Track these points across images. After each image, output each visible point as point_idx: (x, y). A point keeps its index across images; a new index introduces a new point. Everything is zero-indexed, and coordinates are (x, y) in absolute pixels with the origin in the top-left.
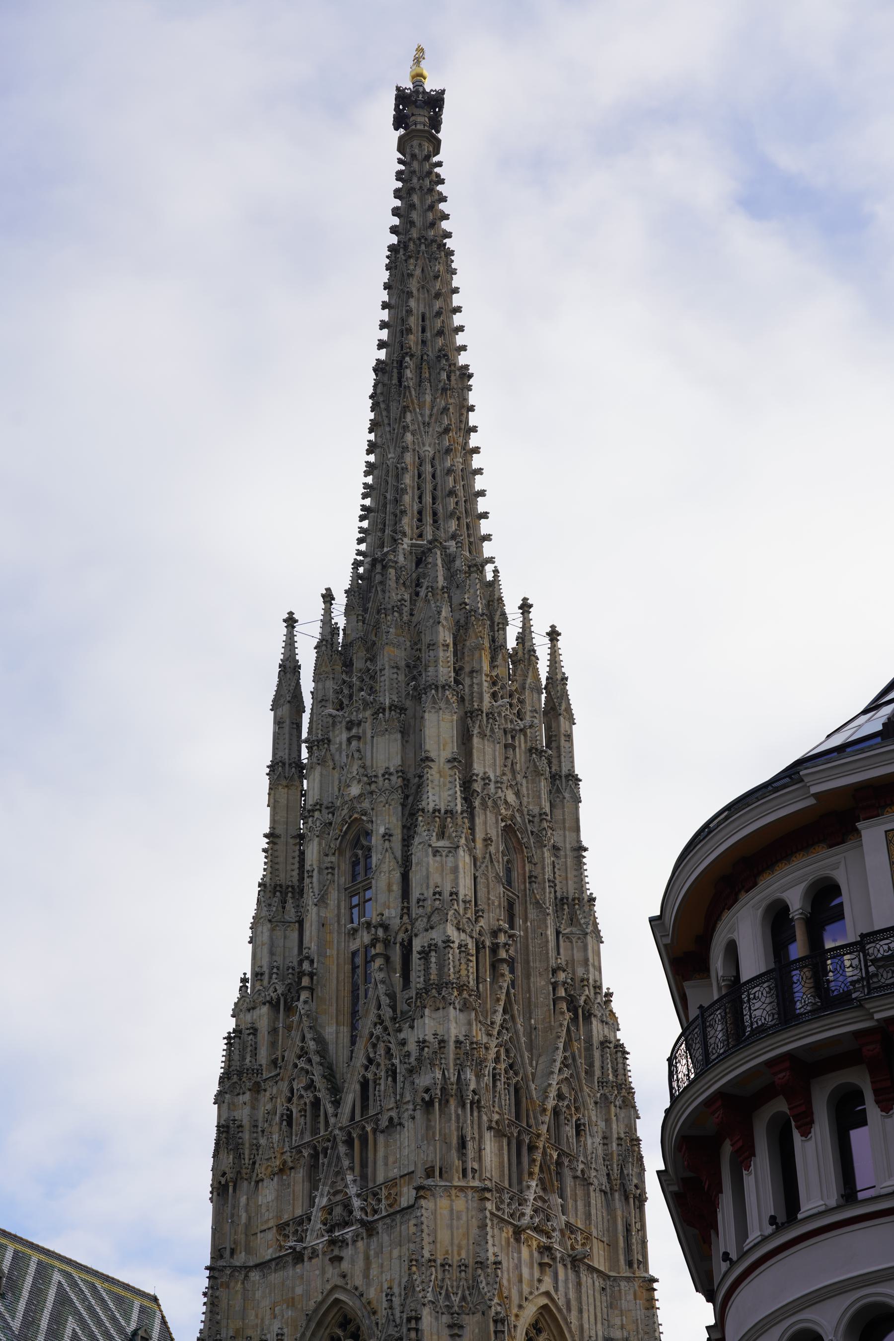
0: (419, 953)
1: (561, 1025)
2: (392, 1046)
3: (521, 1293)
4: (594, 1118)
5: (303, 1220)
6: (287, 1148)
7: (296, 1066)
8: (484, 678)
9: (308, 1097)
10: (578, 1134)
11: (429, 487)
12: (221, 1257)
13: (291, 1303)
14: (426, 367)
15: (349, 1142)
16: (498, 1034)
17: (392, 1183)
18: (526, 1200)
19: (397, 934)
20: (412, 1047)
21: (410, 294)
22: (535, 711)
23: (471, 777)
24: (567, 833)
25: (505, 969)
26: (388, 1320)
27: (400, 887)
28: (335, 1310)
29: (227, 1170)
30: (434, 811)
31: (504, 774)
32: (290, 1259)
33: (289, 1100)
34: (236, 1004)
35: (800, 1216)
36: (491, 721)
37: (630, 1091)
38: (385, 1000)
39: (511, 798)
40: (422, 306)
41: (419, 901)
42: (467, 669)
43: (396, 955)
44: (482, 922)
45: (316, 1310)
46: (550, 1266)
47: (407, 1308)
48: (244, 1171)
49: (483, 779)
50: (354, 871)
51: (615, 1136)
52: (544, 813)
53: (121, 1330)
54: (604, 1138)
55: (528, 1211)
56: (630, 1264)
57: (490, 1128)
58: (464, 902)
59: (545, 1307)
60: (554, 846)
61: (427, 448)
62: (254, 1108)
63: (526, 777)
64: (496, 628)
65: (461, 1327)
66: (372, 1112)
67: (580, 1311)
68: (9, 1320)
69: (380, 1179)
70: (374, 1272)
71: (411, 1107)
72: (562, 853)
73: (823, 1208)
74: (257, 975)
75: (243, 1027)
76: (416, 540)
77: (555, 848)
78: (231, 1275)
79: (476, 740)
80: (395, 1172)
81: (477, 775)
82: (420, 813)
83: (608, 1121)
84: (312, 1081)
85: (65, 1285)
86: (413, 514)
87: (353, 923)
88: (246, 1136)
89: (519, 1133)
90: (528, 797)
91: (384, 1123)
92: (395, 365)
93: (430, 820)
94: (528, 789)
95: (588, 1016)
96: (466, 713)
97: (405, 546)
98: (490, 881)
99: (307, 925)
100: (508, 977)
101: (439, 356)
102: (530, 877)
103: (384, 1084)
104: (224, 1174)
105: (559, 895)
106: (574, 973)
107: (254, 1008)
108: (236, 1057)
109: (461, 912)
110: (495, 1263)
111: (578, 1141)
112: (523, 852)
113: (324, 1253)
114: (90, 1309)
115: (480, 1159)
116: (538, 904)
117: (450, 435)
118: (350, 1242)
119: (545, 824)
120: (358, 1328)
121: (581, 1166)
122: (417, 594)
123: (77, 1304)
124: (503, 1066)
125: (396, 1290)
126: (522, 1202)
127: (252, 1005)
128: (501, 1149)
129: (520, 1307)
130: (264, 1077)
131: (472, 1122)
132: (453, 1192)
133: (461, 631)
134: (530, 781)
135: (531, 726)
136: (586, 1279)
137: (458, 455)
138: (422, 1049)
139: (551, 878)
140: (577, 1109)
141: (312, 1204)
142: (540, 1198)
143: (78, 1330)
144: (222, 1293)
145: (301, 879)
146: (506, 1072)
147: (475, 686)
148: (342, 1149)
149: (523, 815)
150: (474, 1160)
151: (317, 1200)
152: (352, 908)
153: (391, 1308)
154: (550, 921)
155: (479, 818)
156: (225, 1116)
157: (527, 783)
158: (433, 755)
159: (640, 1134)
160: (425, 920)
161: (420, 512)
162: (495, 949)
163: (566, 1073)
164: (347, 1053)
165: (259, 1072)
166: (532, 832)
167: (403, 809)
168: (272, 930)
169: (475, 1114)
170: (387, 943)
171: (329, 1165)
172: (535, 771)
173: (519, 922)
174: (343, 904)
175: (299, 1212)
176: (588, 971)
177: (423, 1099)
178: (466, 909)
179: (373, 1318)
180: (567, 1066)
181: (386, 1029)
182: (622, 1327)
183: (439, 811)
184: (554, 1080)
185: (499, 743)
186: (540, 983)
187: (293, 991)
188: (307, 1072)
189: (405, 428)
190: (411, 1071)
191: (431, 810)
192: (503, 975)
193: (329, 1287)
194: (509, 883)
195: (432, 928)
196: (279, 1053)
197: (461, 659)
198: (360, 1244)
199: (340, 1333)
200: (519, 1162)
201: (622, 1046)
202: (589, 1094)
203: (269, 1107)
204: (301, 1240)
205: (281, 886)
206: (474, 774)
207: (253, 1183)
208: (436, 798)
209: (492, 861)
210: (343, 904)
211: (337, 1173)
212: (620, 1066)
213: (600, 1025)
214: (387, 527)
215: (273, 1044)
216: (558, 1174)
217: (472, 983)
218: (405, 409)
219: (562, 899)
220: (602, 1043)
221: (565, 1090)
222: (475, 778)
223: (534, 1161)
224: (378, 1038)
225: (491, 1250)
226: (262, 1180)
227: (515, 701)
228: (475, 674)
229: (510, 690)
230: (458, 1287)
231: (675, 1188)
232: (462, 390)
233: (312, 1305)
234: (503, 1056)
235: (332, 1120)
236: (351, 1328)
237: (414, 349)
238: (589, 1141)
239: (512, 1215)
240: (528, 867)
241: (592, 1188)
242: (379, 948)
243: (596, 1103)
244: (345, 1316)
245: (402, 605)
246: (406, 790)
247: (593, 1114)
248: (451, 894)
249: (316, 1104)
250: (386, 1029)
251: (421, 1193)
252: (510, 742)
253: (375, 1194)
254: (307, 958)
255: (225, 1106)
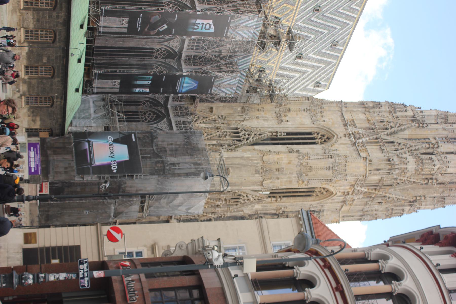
0: (431, 157)
1: (409, 198)
2: (404, 150)
3: (337, 186)
4: (383, 207)
5: (355, 126)
6: (374, 121)
7: (397, 123)
9: (388, 127)
10: (379, 203)
12: (344, 104)
13: (333, 124)
15: (377, 138)
16: (408, 180)
17: (366, 150)
18: (361, 188)
19: (436, 151)
20: (404, 155)
25: (426, 182)
26: (330, 150)
28: (332, 136)
29: (368, 105)
32: (344, 123)
33: (388, 122)
34: (413, 106)
35: (441, 274)
37: (390, 217)
38: (417, 148)
41: (446, 157)
43: (430, 151)
44: (440, 175)
45: (331, 130)
46: (344, 195)
47: (334, 155)
48: (368, 110)
50: (453, 138)
51: (378, 213)
53: (321, 80)
54: (377, 210)
55: (359, 188)
56: (343, 217)
57: (382, 178)
58: (446, 170)
59: (333, 193)
62: (385, 111)
65: (329, 170)
66: (385, 144)
67: (331, 203)
68: (325, 49)
69: (367, 147)
70: (342, 146)
71: (388, 155)
73: (445, 282)
74: (422, 112)
75: (407, 108)
78: (340, 107)
80: (369, 151)
83: (382, 211)
84: (393, 128)
85: (333, 64)
87: (438, 138)
88: (377, 110)
89: (380, 186)
91: (383, 148)
95: (411, 206)
99: (436, 125)
100: (424, 183)
103: (394, 148)
104: (367, 104)
105: (445, 198)
106: (423, 202)
107: (412, 111)
108: (399, 106)
109: (443, 169)
110: (346, 179)
111: (377, 203)
113: (347, 132)
114: (327, 71)
115: (374, 175)
116: (443, 191)
118: (350, 139)
120: (327, 142)
121: (370, 203)
123: (328, 67)
124: (399, 181)
125: (338, 152)
126: (361, 187)
127: (413, 110)
128: (376, 181)
129: (333, 186)
130: (394, 115)
131: (384, 173)
132: (365, 167)
136: (340, 205)
138: (404, 158)
140: (386, 202)
141: (361, 128)
142: (362, 192)
143: (322, 68)
144: (335, 105)
145: (449, 123)
146: (397, 182)
148: (375, 136)
150: (374, 173)
151: (361, 130)
152: (442, 138)
153: (333, 151)
154: (439, 195)
156: (383, 104)
159: (378, 220)
160: (441, 159)
162: (432, 179)
163: (396, 199)
164: (401, 137)
165: (395, 113)
168: (435, 115)
169: (386, 173)
170: (433, 148)
171: (371, 133)
173: (438, 186)
174: (443, 135)
175: (357, 125)
176: (423, 206)
177: (390, 159)
178: (444, 170)
179: (330, 146)
180: (398, 199)
181: (409, 148)
182: (327, 215)
184: (394, 196)
186: (421, 192)
187: (418, 122)
188: (395, 126)
190: (397, 155)
192: (424, 181)
193: (338, 134)
194: (450, 183)
195: (438, 161)
196: (400, 118)
198: (349, 142)
199: (326, 137)
200: (371, 186)
201: (403, 215)
202: (389, 206)
203: (385, 116)
204: (350, 126)
205: (448, 117)
207: (364, 112)
210: (443, 135)
211: (368, 135)
212: (397, 215)
213: (408, 209)
215: (402, 117)
216: (368, 197)
217: (423, 172)
219: (444, 198)
220: (403, 210)
221: (391, 199)
223: (372, 190)
224: (406, 146)
225: (349, 178)
226: (365, 114)
230: (340, 169)
231: (434, 231)
233: (332, 129)
234: (401, 181)
235: (383, 133)
236: (327, 140)
238: (376, 206)
239: (358, 184)
241: (364, 206)
242: (432, 146)
243: (387, 208)
244: (330, 138)
247: (384, 206)
248: (448, 166)
249: (387, 129)
250: (409, 148)
251: (365, 158)
253: (363, 146)
254: (428, 125)
255: (385, 104)
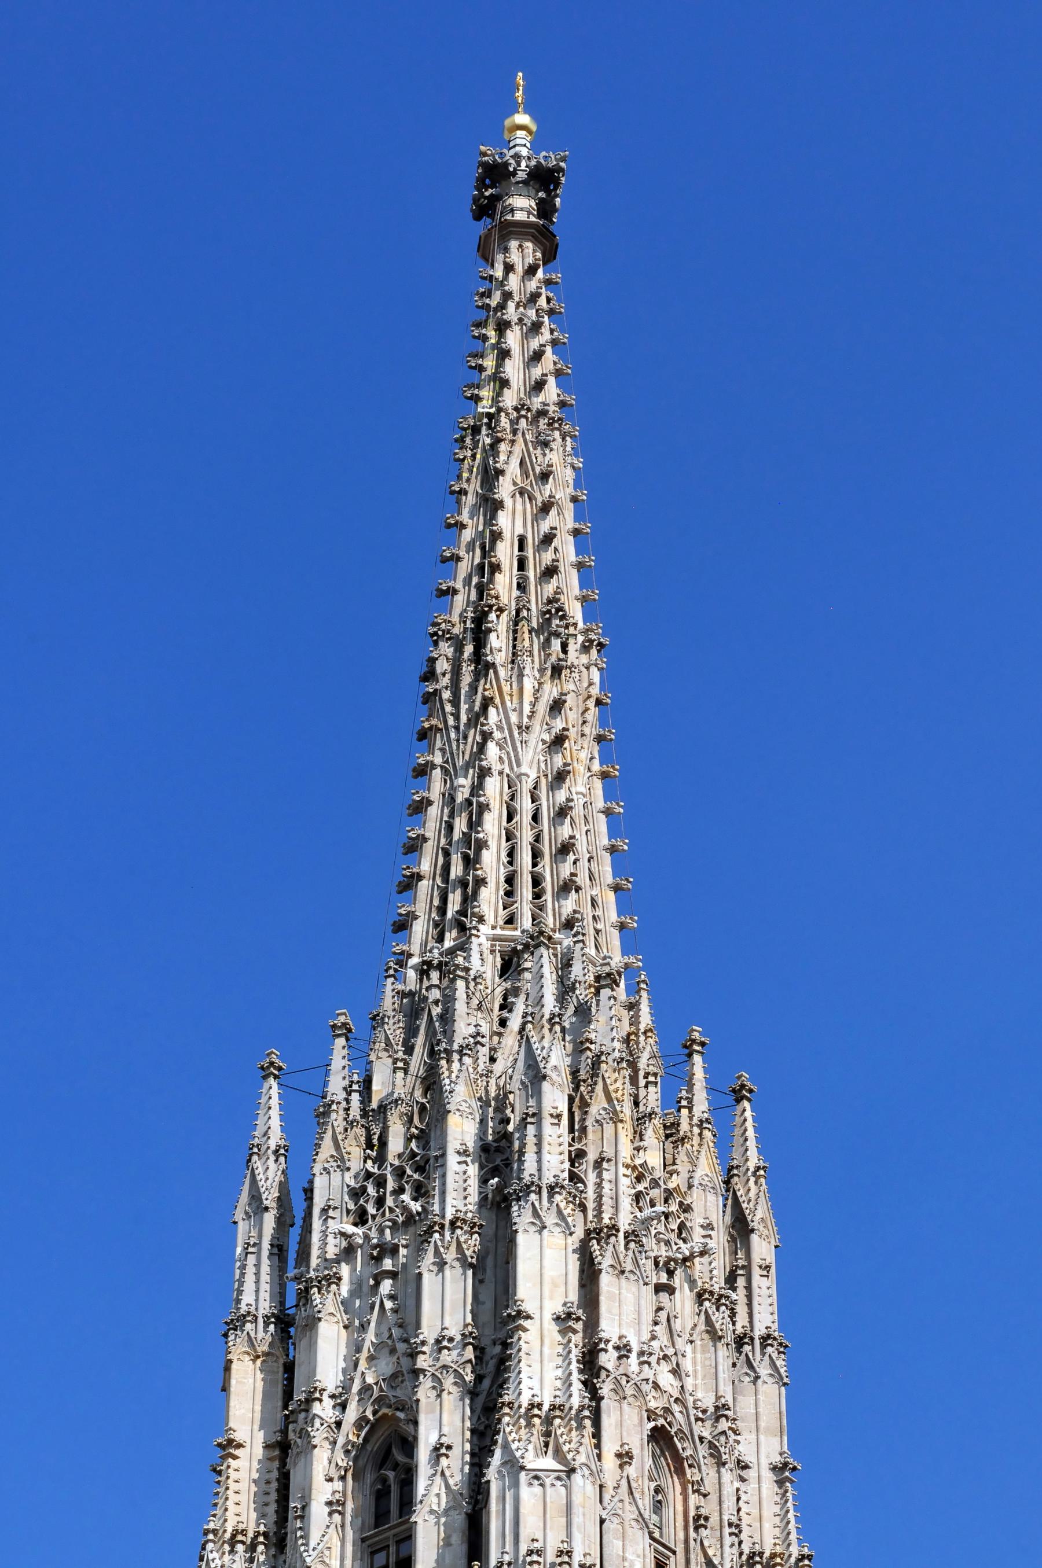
8: (622, 1170)
11: (526, 836)
14: (526, 629)
21: (499, 505)
22: (709, 1227)
23: (597, 1344)
24: (762, 1437)
27: (465, 1539)
30: (532, 1406)
31: (654, 1338)
36: (632, 1245)
39: (666, 1380)
40: (519, 523)
42: (592, 1156)
49: (617, 1348)
52: (724, 1405)
60: (739, 1461)
61: (524, 769)
63: (691, 1342)
64: (642, 1082)
72: (751, 1474)
76: (502, 928)
77: (742, 1466)
79: (607, 1281)
81: (608, 1341)
82: (506, 1410)
86: (498, 883)
90: (695, 1377)
92: (469, 625)
93: (523, 1422)
94: (694, 1363)
96: (588, 1232)
97: (483, 939)
98: (627, 1526)
101: (549, 612)
102: (697, 1518)
105: (746, 1549)
112: (684, 1474)
117: (566, 745)
119: (723, 1425)
122: (503, 1023)
133: (582, 1088)
134: (699, 1348)
135: (702, 1254)
137: (579, 781)
139: (734, 1519)
147: (606, 1185)
149: (686, 1408)
155: (609, 1416)
157: (694, 1351)
158: (529, 1306)
161: (510, 880)
166: (701, 1439)
167: (472, 1400)
172: (707, 1332)
183: (539, 1406)
185: (646, 1284)
189: (486, 736)
191: (525, 1405)
197: (580, 1139)
206: (601, 1340)
208: (535, 1383)
209: (631, 1493)
214: (450, 906)
218: (487, 702)
222: (602, 1346)
227: (674, 1208)
228: (605, 1165)
229: (666, 1190)
232: (588, 668)
237: (504, 600)
240: (694, 1499)
245: (477, 1043)
246: (478, 1368)
248: (560, 1553)
252: (665, 1281)
